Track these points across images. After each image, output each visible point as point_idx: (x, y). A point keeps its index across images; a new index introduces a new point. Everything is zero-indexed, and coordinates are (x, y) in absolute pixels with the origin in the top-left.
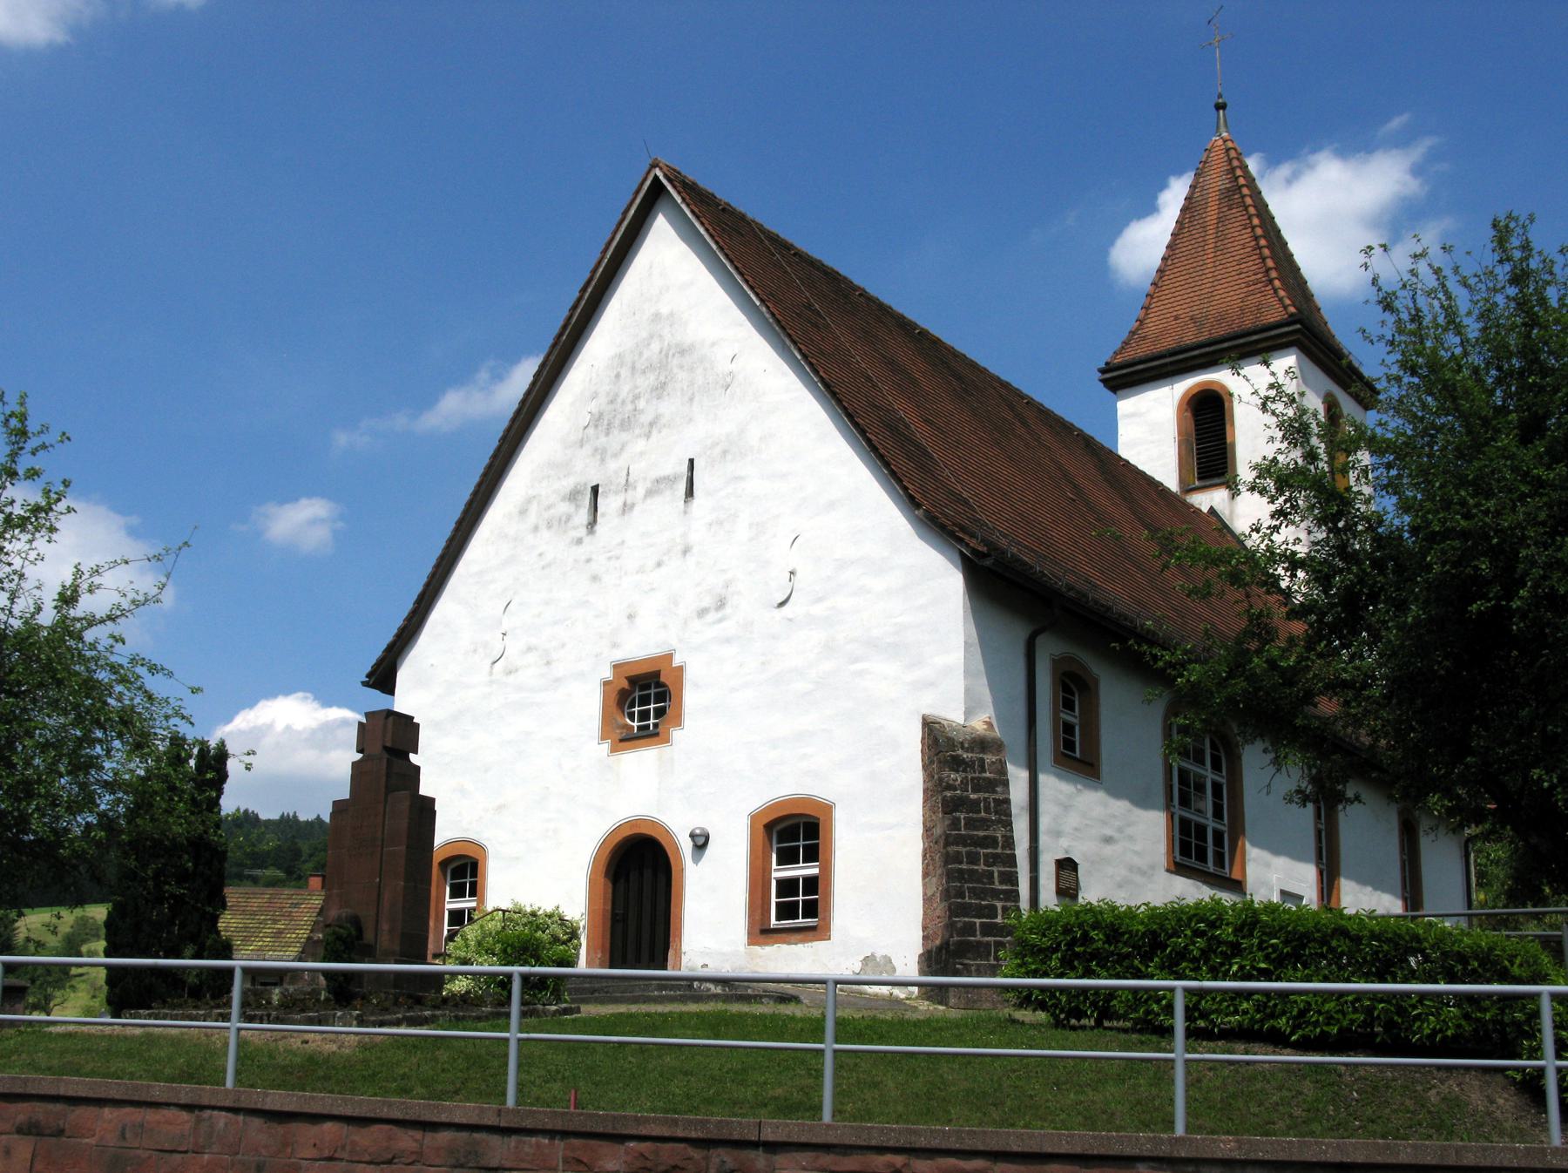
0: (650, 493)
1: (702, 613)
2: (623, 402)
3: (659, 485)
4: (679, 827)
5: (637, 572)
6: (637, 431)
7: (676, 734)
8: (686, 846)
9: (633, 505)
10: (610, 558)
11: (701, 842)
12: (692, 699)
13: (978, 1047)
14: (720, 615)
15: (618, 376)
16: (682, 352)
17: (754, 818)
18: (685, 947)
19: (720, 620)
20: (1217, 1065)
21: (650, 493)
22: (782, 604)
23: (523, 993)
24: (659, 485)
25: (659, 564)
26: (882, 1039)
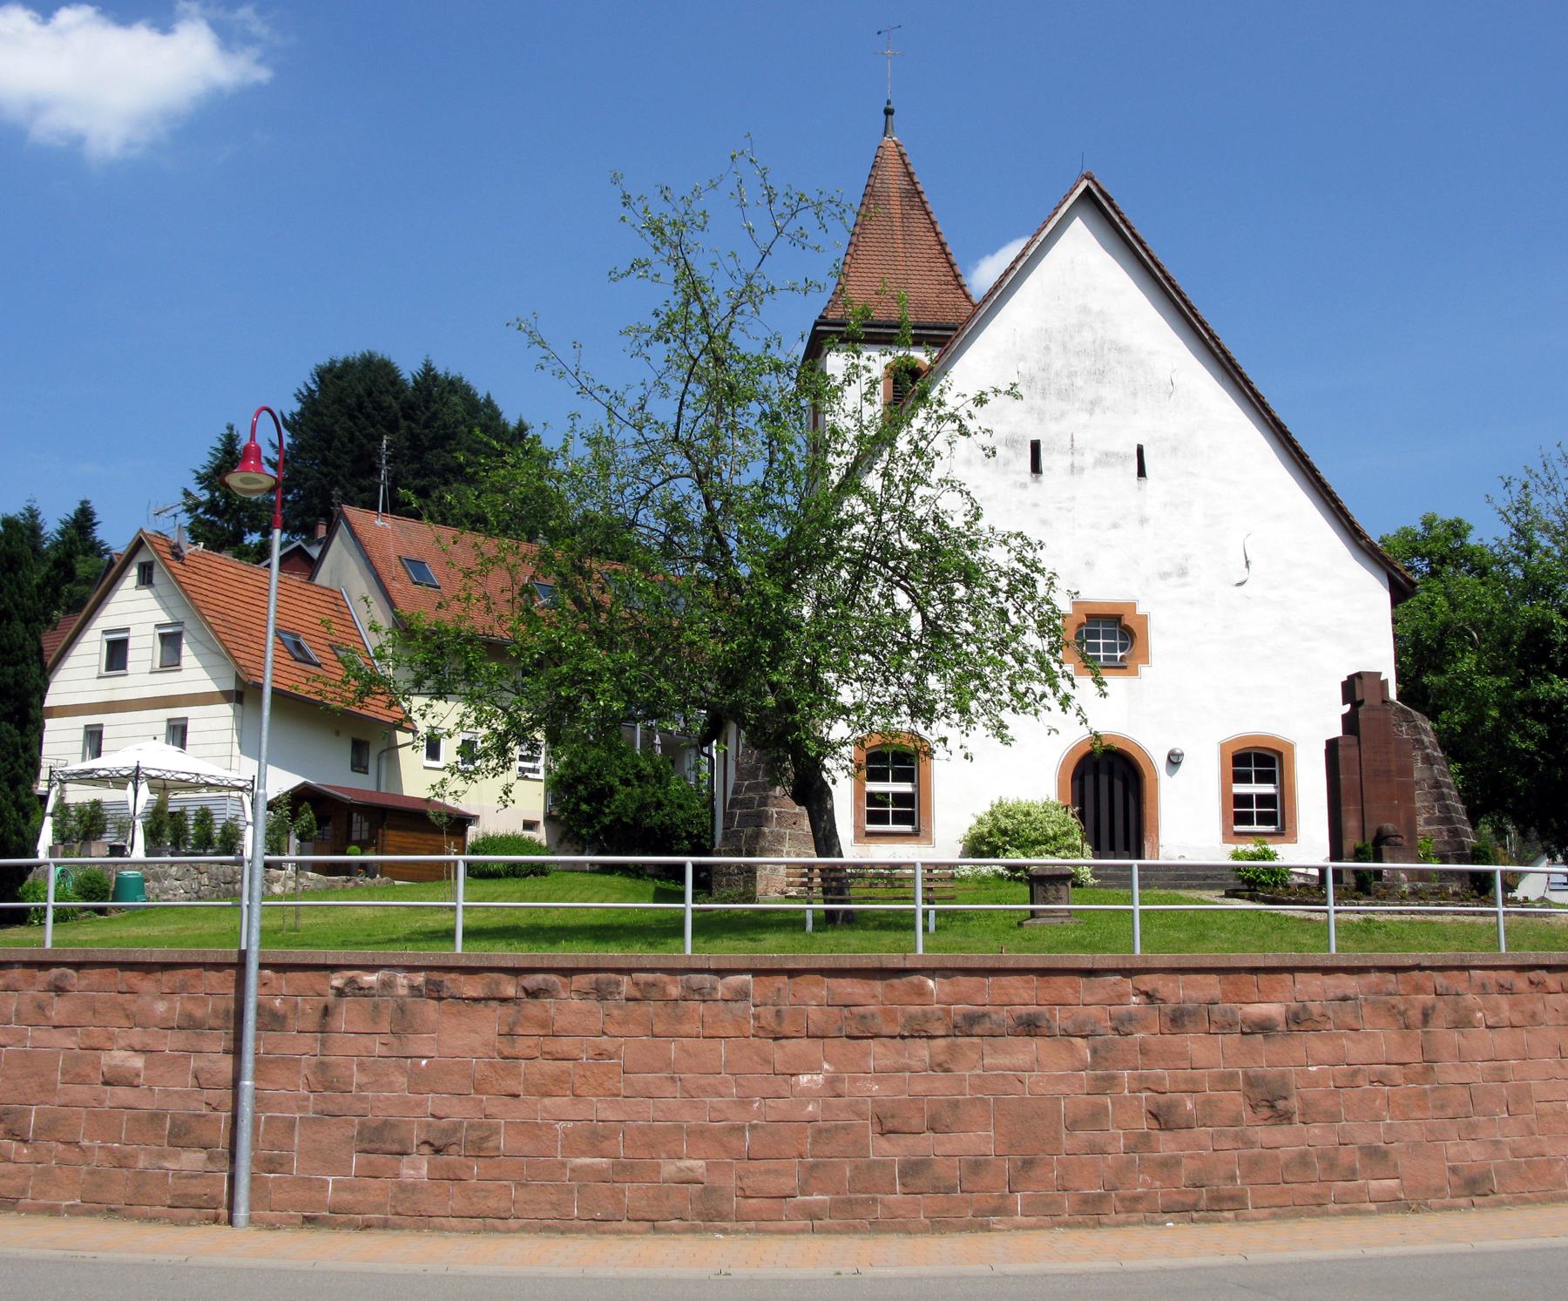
0: (1098, 463)
1: (1164, 576)
2: (1057, 374)
3: (1106, 459)
4: (1153, 746)
5: (1092, 527)
6: (1077, 405)
7: (1143, 669)
8: (1160, 762)
9: (1082, 469)
10: (1060, 509)
11: (1174, 760)
12: (1157, 641)
13: (539, 855)
14: (1183, 580)
15: (1047, 348)
16: (1119, 350)
17: (1223, 747)
18: (1162, 841)
19: (1184, 585)
20: (1248, 914)
21: (1098, 463)
22: (1239, 584)
23: (833, 856)
24: (1106, 459)
25: (1115, 526)
26: (1191, 904)
